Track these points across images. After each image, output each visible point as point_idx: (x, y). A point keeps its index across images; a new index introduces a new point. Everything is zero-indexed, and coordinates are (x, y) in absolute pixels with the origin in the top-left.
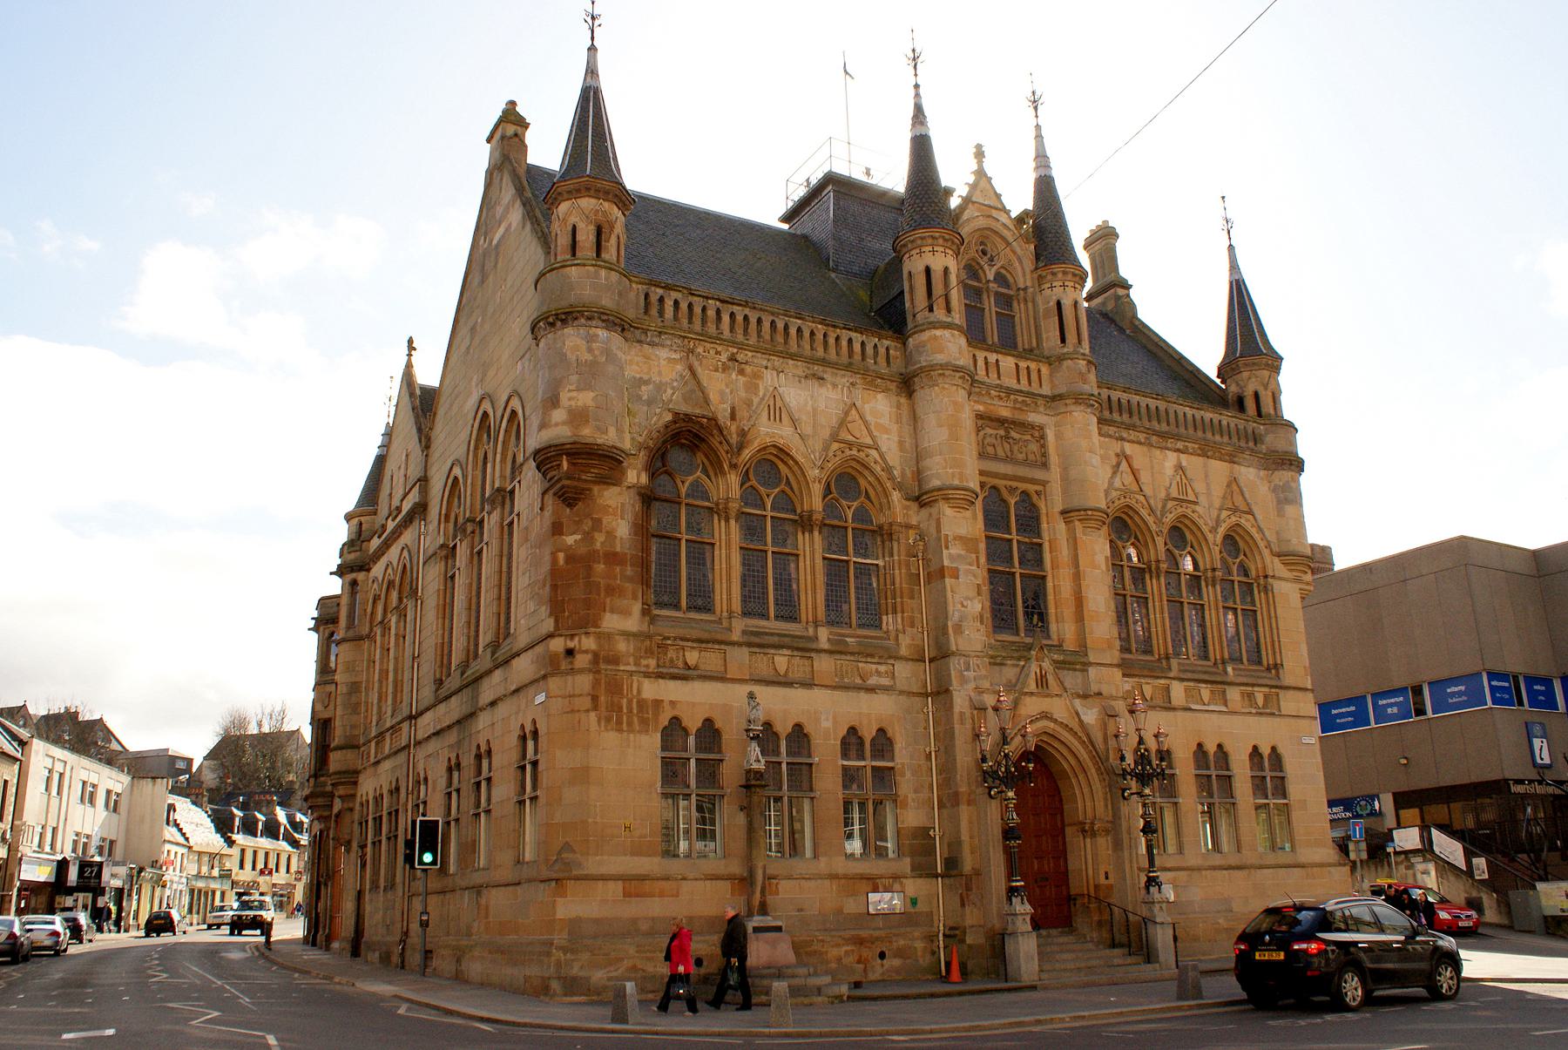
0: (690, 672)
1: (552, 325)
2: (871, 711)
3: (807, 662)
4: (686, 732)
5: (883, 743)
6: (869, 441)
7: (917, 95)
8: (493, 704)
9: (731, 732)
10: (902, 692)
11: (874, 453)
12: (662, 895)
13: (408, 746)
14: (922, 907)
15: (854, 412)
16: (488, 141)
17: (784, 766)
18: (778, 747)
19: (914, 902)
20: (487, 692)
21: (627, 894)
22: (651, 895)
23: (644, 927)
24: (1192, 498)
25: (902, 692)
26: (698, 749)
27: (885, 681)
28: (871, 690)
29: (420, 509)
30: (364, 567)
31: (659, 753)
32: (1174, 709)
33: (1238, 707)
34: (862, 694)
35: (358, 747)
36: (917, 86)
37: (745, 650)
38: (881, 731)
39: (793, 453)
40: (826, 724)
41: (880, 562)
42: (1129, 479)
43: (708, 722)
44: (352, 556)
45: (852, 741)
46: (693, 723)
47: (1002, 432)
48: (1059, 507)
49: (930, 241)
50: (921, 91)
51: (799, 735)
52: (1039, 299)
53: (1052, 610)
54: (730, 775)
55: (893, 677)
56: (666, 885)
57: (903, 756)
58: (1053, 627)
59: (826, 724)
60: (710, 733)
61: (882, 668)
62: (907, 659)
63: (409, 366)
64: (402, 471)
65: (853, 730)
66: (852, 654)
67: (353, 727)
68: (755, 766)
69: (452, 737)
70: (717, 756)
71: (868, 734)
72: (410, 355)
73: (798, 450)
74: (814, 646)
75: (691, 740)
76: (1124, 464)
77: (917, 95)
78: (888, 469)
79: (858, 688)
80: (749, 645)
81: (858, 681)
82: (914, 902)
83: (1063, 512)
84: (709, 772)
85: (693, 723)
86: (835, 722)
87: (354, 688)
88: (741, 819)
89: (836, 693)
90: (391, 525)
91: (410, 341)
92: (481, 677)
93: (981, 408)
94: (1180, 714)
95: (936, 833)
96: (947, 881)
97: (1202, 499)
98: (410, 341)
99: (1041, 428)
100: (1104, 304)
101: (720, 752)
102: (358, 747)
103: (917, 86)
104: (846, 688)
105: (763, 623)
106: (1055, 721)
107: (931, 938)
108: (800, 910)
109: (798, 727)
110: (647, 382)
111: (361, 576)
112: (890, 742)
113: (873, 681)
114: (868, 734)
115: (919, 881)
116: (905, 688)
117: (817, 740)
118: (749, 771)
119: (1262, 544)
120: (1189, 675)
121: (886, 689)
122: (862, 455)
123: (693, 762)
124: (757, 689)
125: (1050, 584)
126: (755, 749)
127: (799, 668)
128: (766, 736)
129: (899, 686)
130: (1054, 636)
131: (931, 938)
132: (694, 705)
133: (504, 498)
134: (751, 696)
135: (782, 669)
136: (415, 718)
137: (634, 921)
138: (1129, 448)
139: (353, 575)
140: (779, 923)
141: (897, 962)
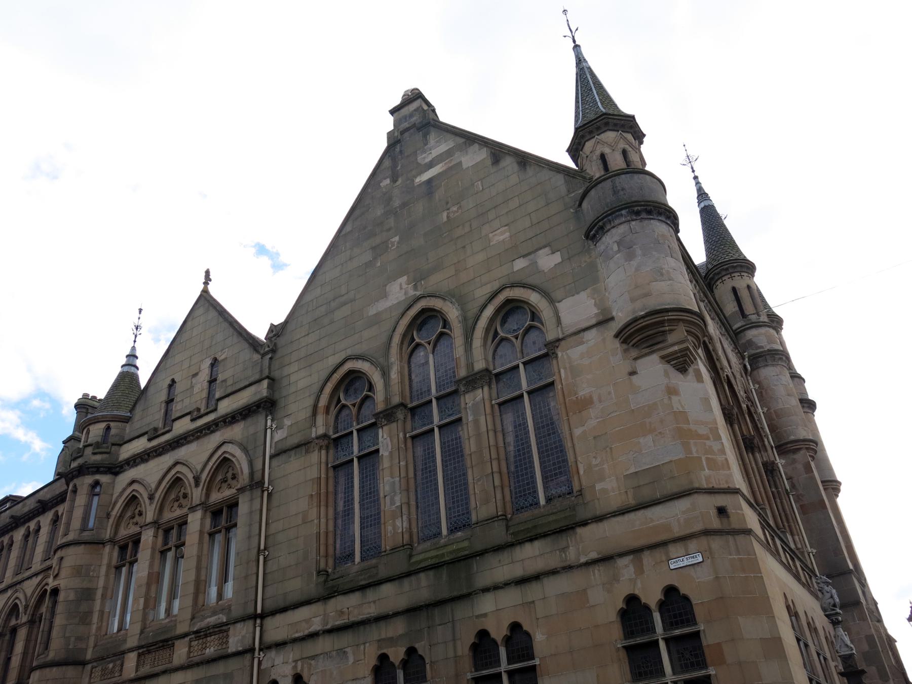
1: (638, 213)
7: (698, 183)
8: (522, 581)
13: (251, 650)
16: (392, 112)
20: (502, 568)
29: (268, 406)
30: (115, 469)
35: (83, 663)
36: (696, 178)
44: (98, 458)
50: (700, 180)
63: (205, 292)
64: (204, 375)
67: (79, 639)
69: (398, 628)
72: (206, 284)
77: (698, 183)
87: (87, 595)
90: (182, 426)
91: (207, 273)
92: (482, 553)
98: (207, 273)
102: (83, 663)
103: (696, 178)
111: (104, 479)
133: (490, 379)
136: (263, 616)
139: (98, 477)
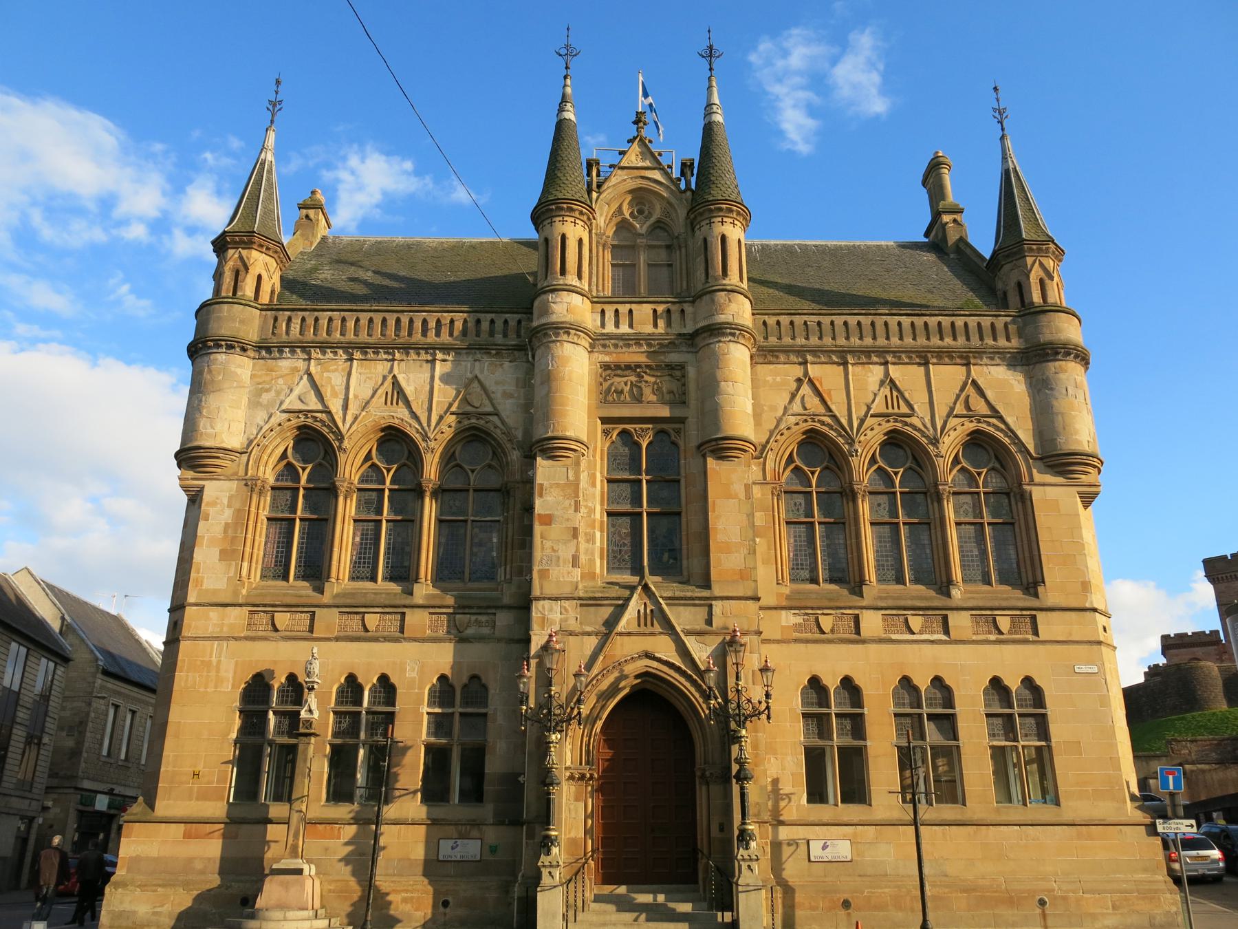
6: (489, 409)
11: (494, 419)
15: (476, 384)
21: (187, 835)
24: (904, 409)
25: (499, 640)
27: (486, 631)
32: (864, 642)
33: (968, 634)
37: (336, 610)
39: (408, 430)
40: (412, 674)
41: (501, 518)
42: (814, 403)
47: (633, 378)
48: (694, 443)
49: (577, 214)
51: (386, 687)
52: (690, 243)
53: (684, 547)
58: (685, 562)
61: (483, 618)
62: (509, 607)
73: (412, 430)
76: (806, 389)
78: (508, 433)
82: (493, 850)
83: (699, 447)
86: (421, 672)
93: (607, 359)
94: (873, 647)
97: (921, 409)
99: (682, 367)
100: (936, 235)
105: (369, 585)
106: (659, 660)
109: (384, 679)
110: (267, 391)
112: (485, 687)
119: (1013, 448)
120: (890, 603)
121: (480, 639)
122: (482, 422)
125: (684, 520)
130: (685, 573)
137: (190, 860)
138: (813, 370)
141: (461, 912)
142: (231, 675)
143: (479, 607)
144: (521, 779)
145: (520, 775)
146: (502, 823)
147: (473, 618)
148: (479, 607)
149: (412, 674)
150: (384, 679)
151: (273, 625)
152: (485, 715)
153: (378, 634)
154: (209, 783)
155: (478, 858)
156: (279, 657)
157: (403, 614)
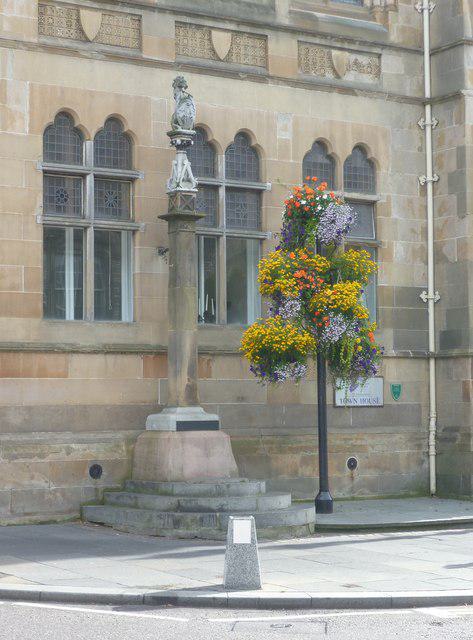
0: (87, 46)
2: (346, 120)
3: (258, 43)
4: (79, 134)
5: (363, 167)
9: (150, 136)
10: (391, 96)
12: (43, 373)
14: (406, 399)
17: (222, 192)
18: (214, 164)
19: (396, 391)
22: (27, 374)
23: (15, 419)
25: (391, 96)
26: (98, 162)
27: (367, 79)
28: (347, 90)
31: (40, 165)
34: (336, 97)
37: (171, 19)
38: (360, 148)
43: (114, 121)
45: (319, 159)
46: (91, 122)
54: (148, 197)
55: (378, 74)
56: (49, 360)
57: (389, 188)
59: (284, 135)
60: (116, 138)
61: (364, 60)
65: (321, 145)
66: (324, 36)
68: (184, 187)
70: (127, 173)
71: (342, 150)
74: (269, 20)
75: (88, 147)
79: (330, 87)
80: (175, 12)
81: (330, 76)
82: (396, 391)
84: (114, 192)
85: (91, 122)
86: (296, 133)
88: (161, 267)
89: (300, 92)
95: (430, 295)
96: (442, 363)
101: (129, 167)
104: (313, 85)
107: (419, 440)
108: (242, 399)
109: (244, 136)
112: (372, 164)
113: (350, 78)
114: (342, 150)
115: (405, 363)
116: (395, 90)
117: (270, 159)
118: (173, 196)
121: (367, 91)
123: (90, 180)
124: (187, 76)
126: (182, 164)
127: (247, 53)
128: (197, 143)
129: (387, 85)
131: (419, 440)
132: (92, 94)
134: (179, 85)
135: (222, 52)
140: (214, 417)
141: (371, 475)
142: (25, 108)
143: (363, 43)
144: (423, 296)
145: (421, 290)
146: (406, 357)
147: (353, 57)
148: (363, 43)
149: (287, 136)
150: (244, 136)
151: (81, 31)
152: (372, 204)
153: (232, 66)
154: (13, 287)
155: (381, 403)
156: (97, 87)
157: (264, 38)
